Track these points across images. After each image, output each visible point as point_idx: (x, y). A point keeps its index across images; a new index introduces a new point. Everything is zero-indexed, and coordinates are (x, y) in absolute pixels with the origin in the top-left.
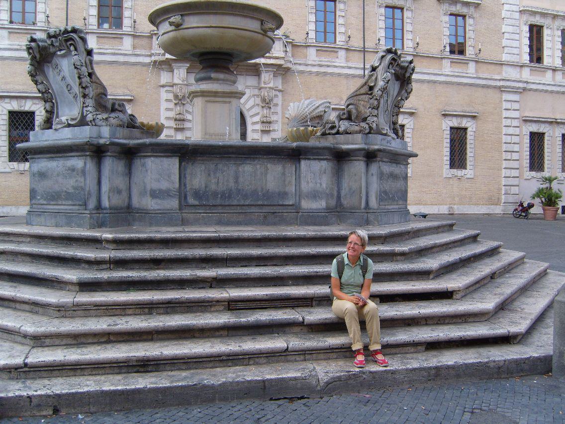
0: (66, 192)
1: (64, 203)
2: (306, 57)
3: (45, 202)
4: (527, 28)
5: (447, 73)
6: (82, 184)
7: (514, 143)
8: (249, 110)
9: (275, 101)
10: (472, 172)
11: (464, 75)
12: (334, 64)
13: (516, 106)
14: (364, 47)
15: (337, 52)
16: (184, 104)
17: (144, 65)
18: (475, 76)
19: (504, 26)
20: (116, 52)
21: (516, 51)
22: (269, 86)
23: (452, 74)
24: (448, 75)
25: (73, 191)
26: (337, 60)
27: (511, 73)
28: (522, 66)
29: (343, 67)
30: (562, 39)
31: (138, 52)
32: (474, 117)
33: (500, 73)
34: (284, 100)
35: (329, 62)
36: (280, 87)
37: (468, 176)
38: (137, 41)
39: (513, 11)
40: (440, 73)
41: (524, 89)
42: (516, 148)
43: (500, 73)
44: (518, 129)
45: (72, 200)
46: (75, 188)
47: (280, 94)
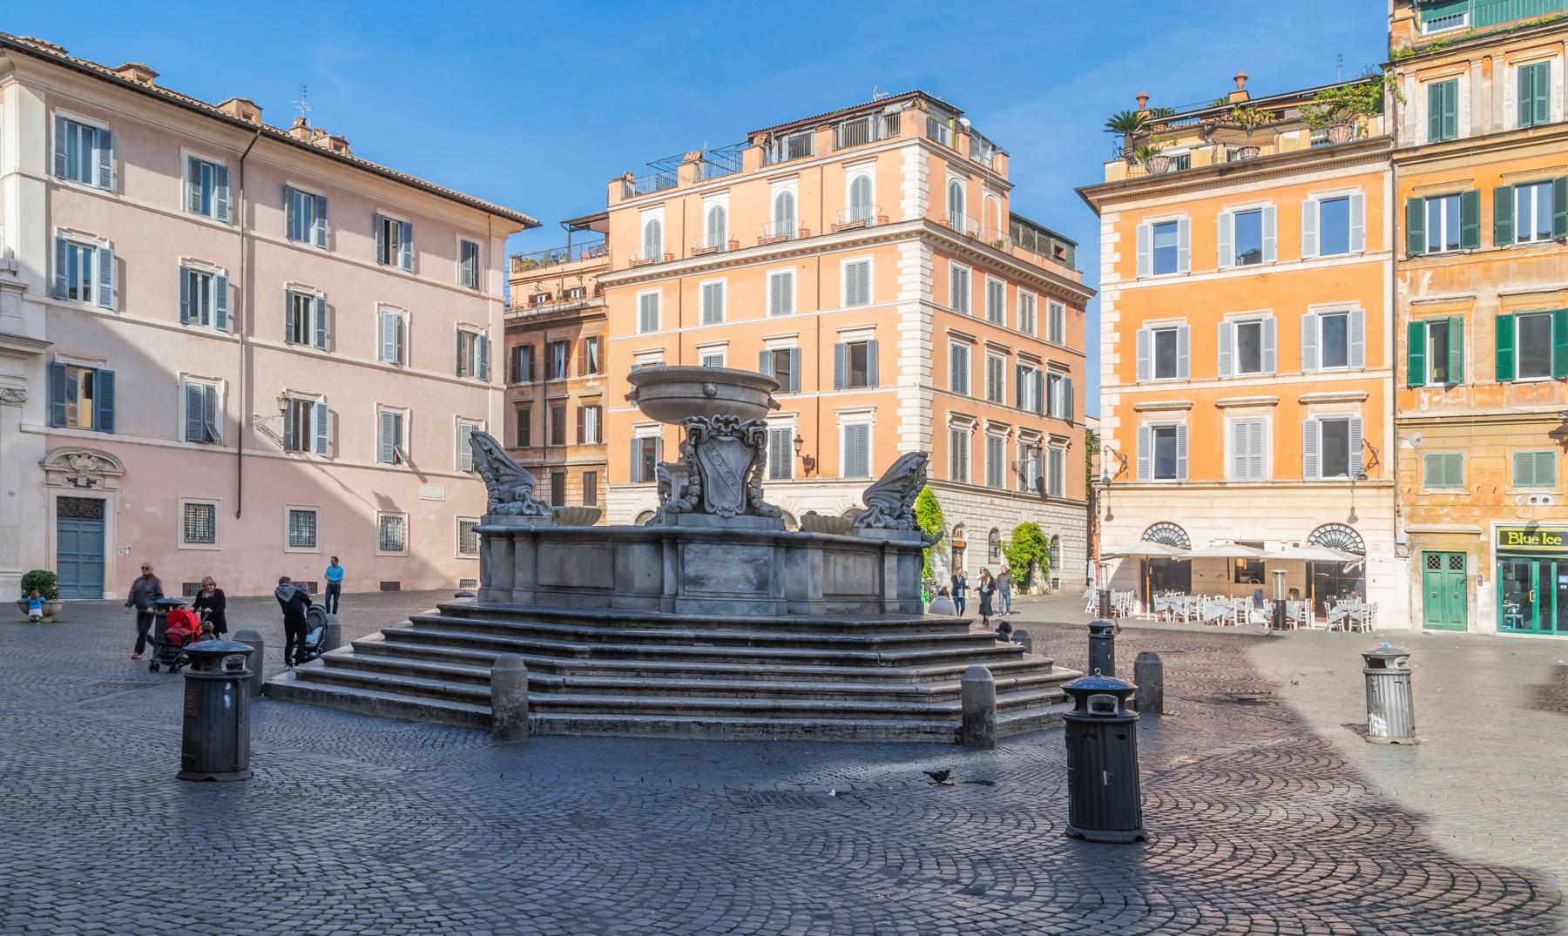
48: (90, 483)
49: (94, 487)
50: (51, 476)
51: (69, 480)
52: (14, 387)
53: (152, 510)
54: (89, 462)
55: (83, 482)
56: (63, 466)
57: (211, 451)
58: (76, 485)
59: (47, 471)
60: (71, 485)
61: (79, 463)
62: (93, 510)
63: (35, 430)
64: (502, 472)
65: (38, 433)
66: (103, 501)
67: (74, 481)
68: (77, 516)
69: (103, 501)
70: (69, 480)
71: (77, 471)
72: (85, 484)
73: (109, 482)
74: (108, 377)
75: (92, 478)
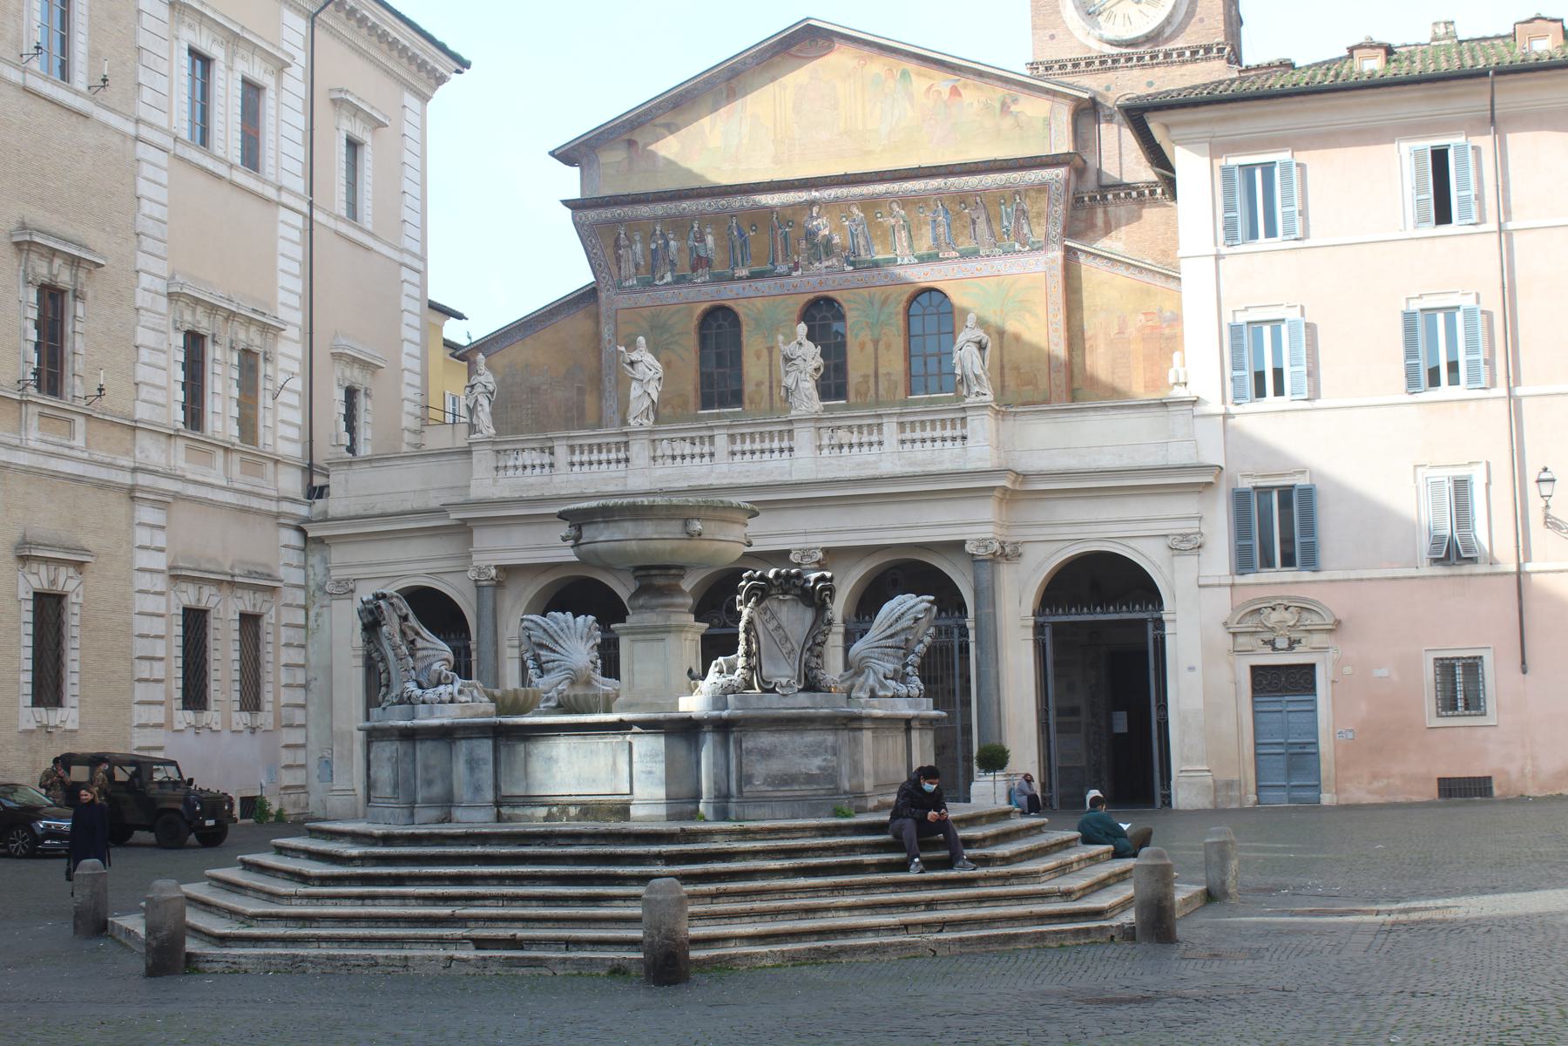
0: (806, 774)
1: (803, 787)
3: (770, 789)
4: (179, 340)
5: (32, 444)
6: (835, 764)
7: (156, 637)
11: (67, 452)
13: (160, 539)
18: (85, 455)
19: (139, 329)
21: (159, 397)
23: (43, 447)
24: (34, 451)
25: (818, 772)
27: (151, 452)
28: (170, 435)
30: (241, 374)
32: (79, 565)
33: (129, 452)
39: (157, 293)
41: (177, 496)
42: (159, 649)
43: (129, 452)
44: (162, 600)
45: (818, 784)
46: (820, 768)
48: (1292, 645)
49: (1298, 648)
50: (1240, 639)
51: (1265, 643)
52: (1188, 531)
53: (1383, 672)
54: (1287, 615)
55: (1282, 643)
56: (1250, 624)
57: (1471, 575)
58: (1274, 649)
59: (1234, 634)
60: (1268, 649)
61: (1274, 617)
62: (1299, 679)
63: (1216, 581)
64: (543, 659)
65: (1220, 586)
66: (1312, 667)
67: (1272, 643)
68: (1279, 691)
69: (1312, 667)
70: (1265, 643)
71: (1272, 629)
72: (1285, 645)
73: (1318, 640)
74: (1308, 493)
75: (1295, 636)
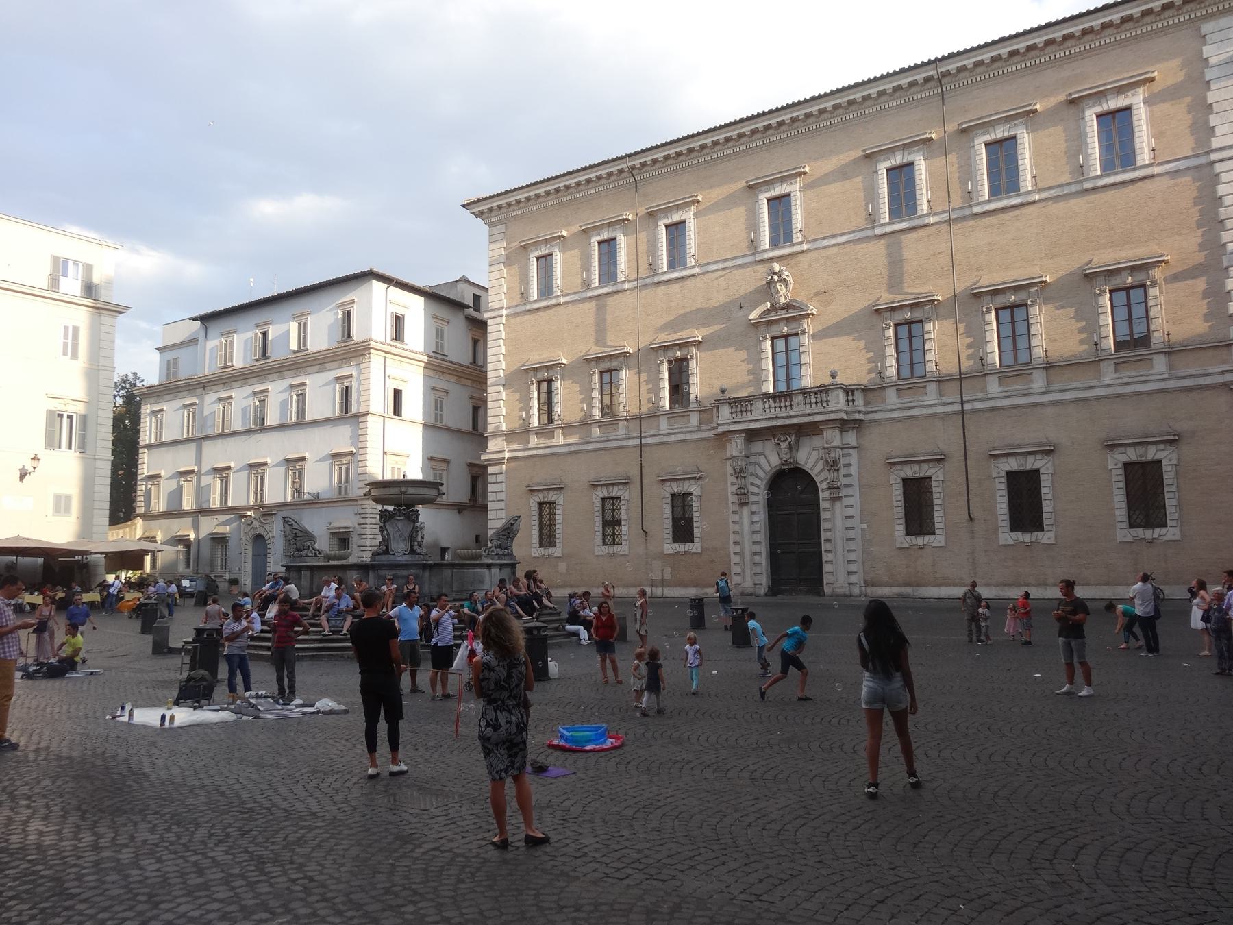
2: (885, 401)
8: (818, 474)
9: (842, 461)
10: (1176, 531)
12: (921, 403)
14: (960, 374)
15: (925, 387)
16: (745, 477)
17: (709, 439)
20: (684, 430)
22: (833, 445)
24: (1109, 386)
26: (926, 398)
29: (935, 405)
31: (704, 427)
34: (860, 458)
35: (914, 402)
36: (854, 443)
37: (1168, 537)
38: (703, 415)
40: (1097, 384)
47: (854, 452)
